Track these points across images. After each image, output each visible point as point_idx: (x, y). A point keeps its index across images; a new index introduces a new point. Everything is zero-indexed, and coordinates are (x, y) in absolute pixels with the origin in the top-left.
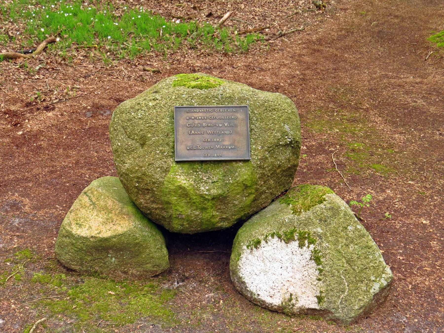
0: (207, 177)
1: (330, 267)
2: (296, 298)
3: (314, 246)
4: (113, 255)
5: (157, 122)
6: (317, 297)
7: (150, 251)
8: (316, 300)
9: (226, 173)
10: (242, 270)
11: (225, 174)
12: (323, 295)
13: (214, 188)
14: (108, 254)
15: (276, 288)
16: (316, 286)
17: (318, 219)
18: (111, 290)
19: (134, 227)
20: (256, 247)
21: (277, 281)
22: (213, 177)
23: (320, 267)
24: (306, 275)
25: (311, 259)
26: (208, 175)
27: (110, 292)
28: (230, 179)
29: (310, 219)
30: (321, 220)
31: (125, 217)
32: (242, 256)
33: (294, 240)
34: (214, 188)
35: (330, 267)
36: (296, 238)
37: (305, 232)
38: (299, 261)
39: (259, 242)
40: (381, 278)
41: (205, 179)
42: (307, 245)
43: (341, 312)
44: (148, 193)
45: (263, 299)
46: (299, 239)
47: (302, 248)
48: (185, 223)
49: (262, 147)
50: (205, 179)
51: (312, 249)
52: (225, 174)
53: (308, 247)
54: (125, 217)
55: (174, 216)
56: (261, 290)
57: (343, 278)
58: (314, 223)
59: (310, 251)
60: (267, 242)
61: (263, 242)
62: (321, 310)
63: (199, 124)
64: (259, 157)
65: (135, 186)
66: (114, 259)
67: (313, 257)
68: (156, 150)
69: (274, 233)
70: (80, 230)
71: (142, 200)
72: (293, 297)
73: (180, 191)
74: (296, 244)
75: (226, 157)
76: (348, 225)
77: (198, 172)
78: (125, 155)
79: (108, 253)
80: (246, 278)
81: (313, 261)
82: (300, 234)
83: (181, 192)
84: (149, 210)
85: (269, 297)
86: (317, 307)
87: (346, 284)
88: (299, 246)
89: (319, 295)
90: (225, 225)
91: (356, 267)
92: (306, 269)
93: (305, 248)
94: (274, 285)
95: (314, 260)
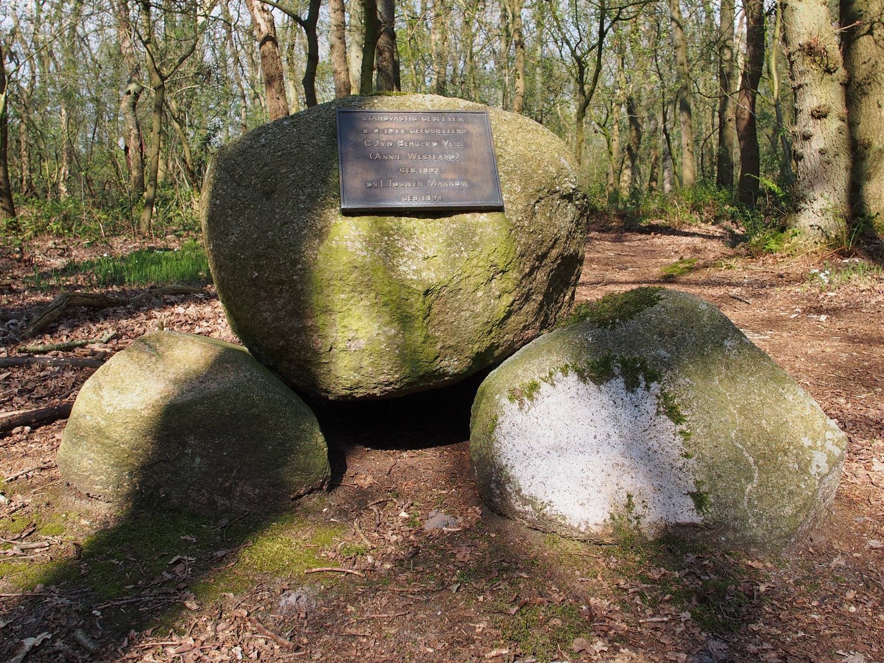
0: (413, 247)
1: (705, 427)
2: (644, 502)
3: (660, 386)
4: (198, 450)
5: (299, 145)
6: (693, 495)
7: (285, 435)
8: (690, 502)
9: (452, 239)
10: (504, 450)
11: (449, 241)
12: (704, 488)
13: (429, 269)
14: (184, 448)
15: (590, 482)
16: (684, 470)
17: (655, 334)
18: (189, 532)
19: (249, 380)
20: (530, 397)
21: (591, 467)
22: (425, 248)
23: (683, 427)
24: (655, 448)
25: (658, 413)
26: (414, 243)
27: (188, 538)
28: (463, 249)
29: (639, 333)
30: (661, 334)
31: (229, 366)
32: (500, 419)
33: (613, 376)
34: (429, 269)
35: (705, 427)
36: (617, 371)
37: (635, 359)
38: (633, 419)
39: (534, 387)
40: (825, 441)
41: (410, 250)
42: (643, 384)
43: (755, 525)
44: (281, 292)
45: (563, 510)
46: (623, 374)
47: (633, 392)
48: (364, 363)
49: (524, 188)
50: (410, 250)
51: (657, 391)
52: (449, 241)
53: (648, 388)
54: (229, 366)
55: (341, 346)
56: (556, 491)
57: (741, 446)
58: (648, 342)
59: (654, 397)
60: (553, 385)
61: (545, 387)
62: (706, 525)
63: (390, 141)
64: (520, 207)
65: (253, 280)
66: (198, 460)
67: (661, 409)
68: (298, 195)
69: (567, 366)
70: (120, 397)
71: (266, 315)
72: (634, 499)
73: (354, 275)
74: (619, 383)
75: (454, 201)
76: (723, 339)
77: (392, 235)
78: (229, 219)
79: (185, 445)
80: (518, 467)
81: (665, 416)
82: (624, 363)
83: (356, 278)
84: (283, 337)
85: (577, 505)
86: (697, 519)
87: (751, 460)
88: (627, 388)
89: (695, 490)
90: (453, 365)
91: (764, 421)
92: (652, 435)
93: (640, 391)
94: (585, 475)
95: (666, 413)
